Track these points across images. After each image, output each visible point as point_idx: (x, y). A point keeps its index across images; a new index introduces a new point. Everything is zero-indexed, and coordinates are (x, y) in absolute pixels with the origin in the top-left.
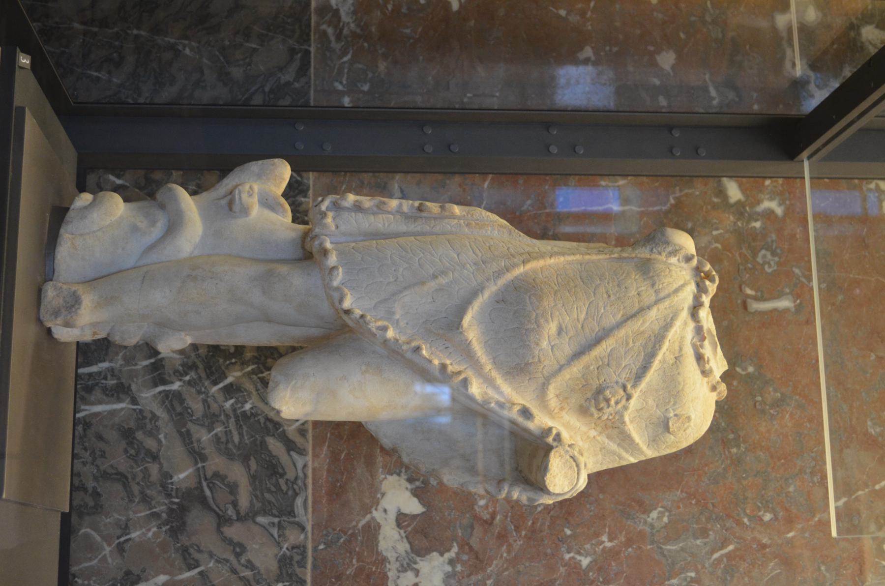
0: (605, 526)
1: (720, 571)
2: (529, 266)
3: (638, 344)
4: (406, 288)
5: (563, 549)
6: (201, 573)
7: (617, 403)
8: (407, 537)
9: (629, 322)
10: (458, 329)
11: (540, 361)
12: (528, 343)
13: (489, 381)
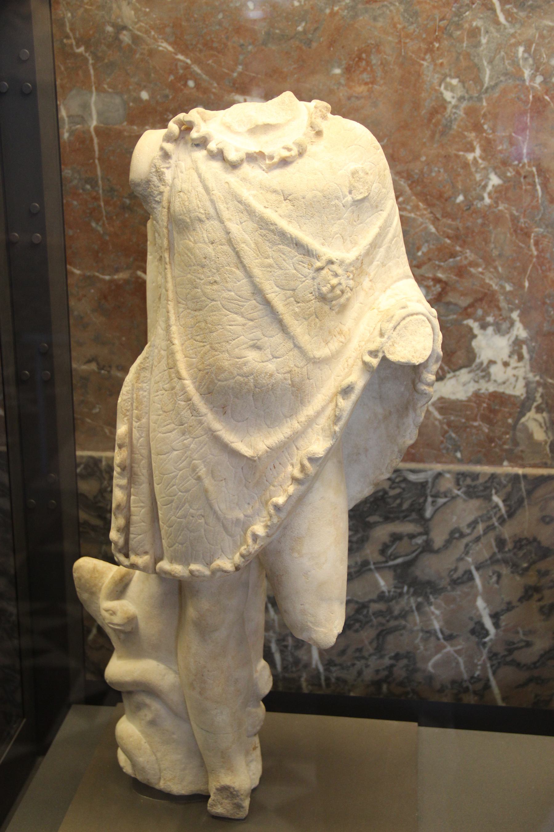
0: (457, 156)
1: (521, 14)
2: (184, 373)
3: (270, 252)
4: (211, 507)
5: (479, 206)
6: (477, 569)
7: (336, 275)
8: (454, 371)
9: (246, 262)
10: (255, 461)
11: (290, 372)
12: (270, 386)
13: (311, 422)
